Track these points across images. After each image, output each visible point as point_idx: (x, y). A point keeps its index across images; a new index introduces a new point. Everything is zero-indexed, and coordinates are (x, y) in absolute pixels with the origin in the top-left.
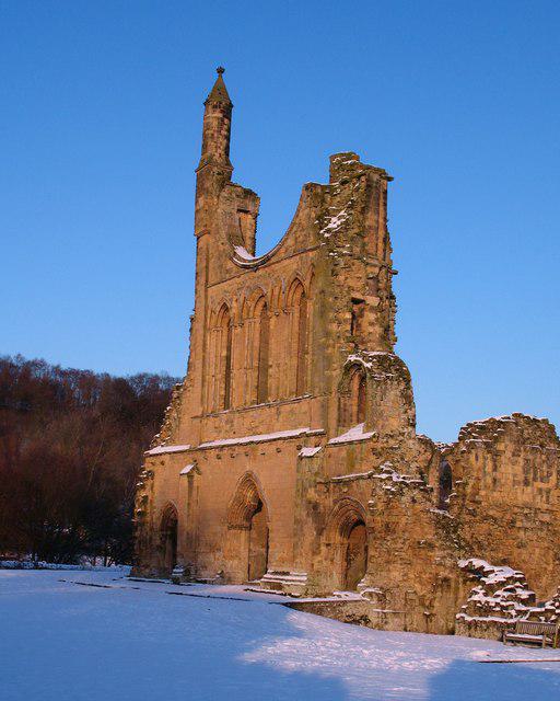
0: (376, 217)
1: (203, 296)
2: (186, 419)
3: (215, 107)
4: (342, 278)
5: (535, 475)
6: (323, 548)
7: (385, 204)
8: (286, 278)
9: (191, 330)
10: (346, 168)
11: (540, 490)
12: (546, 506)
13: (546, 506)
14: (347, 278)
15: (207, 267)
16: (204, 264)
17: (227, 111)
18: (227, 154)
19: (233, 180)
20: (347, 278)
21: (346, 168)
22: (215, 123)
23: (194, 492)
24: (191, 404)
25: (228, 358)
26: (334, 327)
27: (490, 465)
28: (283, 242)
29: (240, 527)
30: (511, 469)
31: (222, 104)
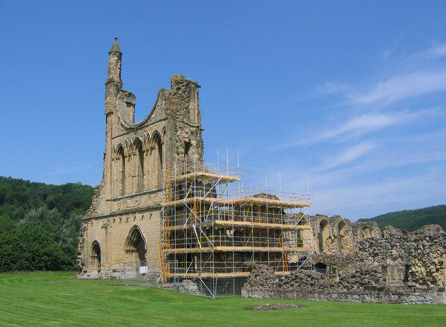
1: (110, 143)
2: (103, 203)
4: (179, 133)
8: (151, 133)
15: (111, 129)
17: (120, 56)
18: (120, 76)
24: (106, 194)
25: (123, 172)
26: (176, 155)
28: (149, 117)
29: (133, 251)
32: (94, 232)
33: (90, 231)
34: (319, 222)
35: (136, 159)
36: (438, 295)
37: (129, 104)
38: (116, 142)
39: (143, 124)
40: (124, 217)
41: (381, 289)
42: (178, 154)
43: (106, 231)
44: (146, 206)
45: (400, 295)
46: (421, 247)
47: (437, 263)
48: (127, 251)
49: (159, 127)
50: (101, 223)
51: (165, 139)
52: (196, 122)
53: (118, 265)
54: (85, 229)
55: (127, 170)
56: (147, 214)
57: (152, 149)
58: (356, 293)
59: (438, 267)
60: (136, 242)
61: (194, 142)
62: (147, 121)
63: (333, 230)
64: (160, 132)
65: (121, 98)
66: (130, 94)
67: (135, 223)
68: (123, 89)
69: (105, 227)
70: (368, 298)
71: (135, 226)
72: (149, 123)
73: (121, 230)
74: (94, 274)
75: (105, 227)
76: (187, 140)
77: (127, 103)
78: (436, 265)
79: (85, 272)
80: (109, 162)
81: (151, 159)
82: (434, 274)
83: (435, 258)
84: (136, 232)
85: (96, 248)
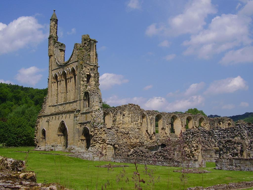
0: (93, 52)
1: (51, 73)
2: (47, 107)
3: (53, 21)
4: (84, 69)
5: (134, 119)
6: (81, 141)
7: (96, 49)
9: (48, 82)
11: (136, 123)
12: (137, 127)
13: (137, 127)
14: (85, 69)
16: (51, 64)
17: (56, 21)
18: (57, 33)
19: (59, 41)
20: (85, 69)
22: (53, 25)
23: (50, 126)
26: (82, 82)
27: (122, 117)
28: (70, 59)
29: (61, 135)
32: (42, 124)
33: (41, 123)
34: (186, 118)
35: (63, 83)
36: (194, 163)
37: (61, 50)
38: (54, 73)
39: (67, 63)
40: (57, 116)
41: (170, 159)
42: (83, 82)
43: (48, 124)
44: (68, 110)
45: (178, 162)
46: (188, 138)
47: (195, 146)
48: (59, 135)
49: (74, 66)
50: (46, 119)
51: (77, 73)
52: (94, 62)
53: (54, 143)
54: (39, 122)
55: (59, 89)
57: (71, 78)
58: (160, 161)
59: (195, 148)
60: (63, 130)
61: (92, 75)
62: (68, 62)
63: (195, 123)
65: (57, 47)
66: (62, 44)
67: (63, 120)
68: (59, 41)
69: (48, 121)
70: (165, 164)
71: (63, 121)
72: (70, 63)
73: (55, 123)
74: (43, 148)
75: (48, 121)
76: (88, 73)
77: (60, 49)
78: (194, 148)
79: (39, 146)
80: (50, 84)
81: (71, 84)
82: (193, 152)
83: (194, 144)
84: (63, 124)
85: (44, 132)
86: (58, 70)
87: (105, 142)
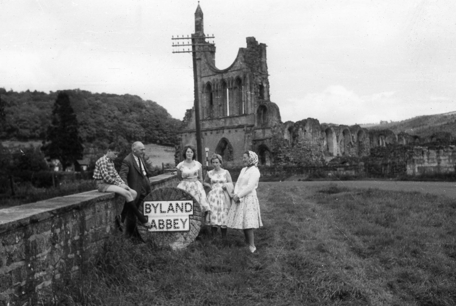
10: (251, 41)
21: (251, 41)
28: (232, 66)
30: (309, 135)
31: (199, 14)
56: (233, 131)
61: (265, 85)
64: (241, 76)
67: (223, 136)
76: (260, 84)
86: (212, 78)
87: (289, 160)
